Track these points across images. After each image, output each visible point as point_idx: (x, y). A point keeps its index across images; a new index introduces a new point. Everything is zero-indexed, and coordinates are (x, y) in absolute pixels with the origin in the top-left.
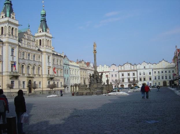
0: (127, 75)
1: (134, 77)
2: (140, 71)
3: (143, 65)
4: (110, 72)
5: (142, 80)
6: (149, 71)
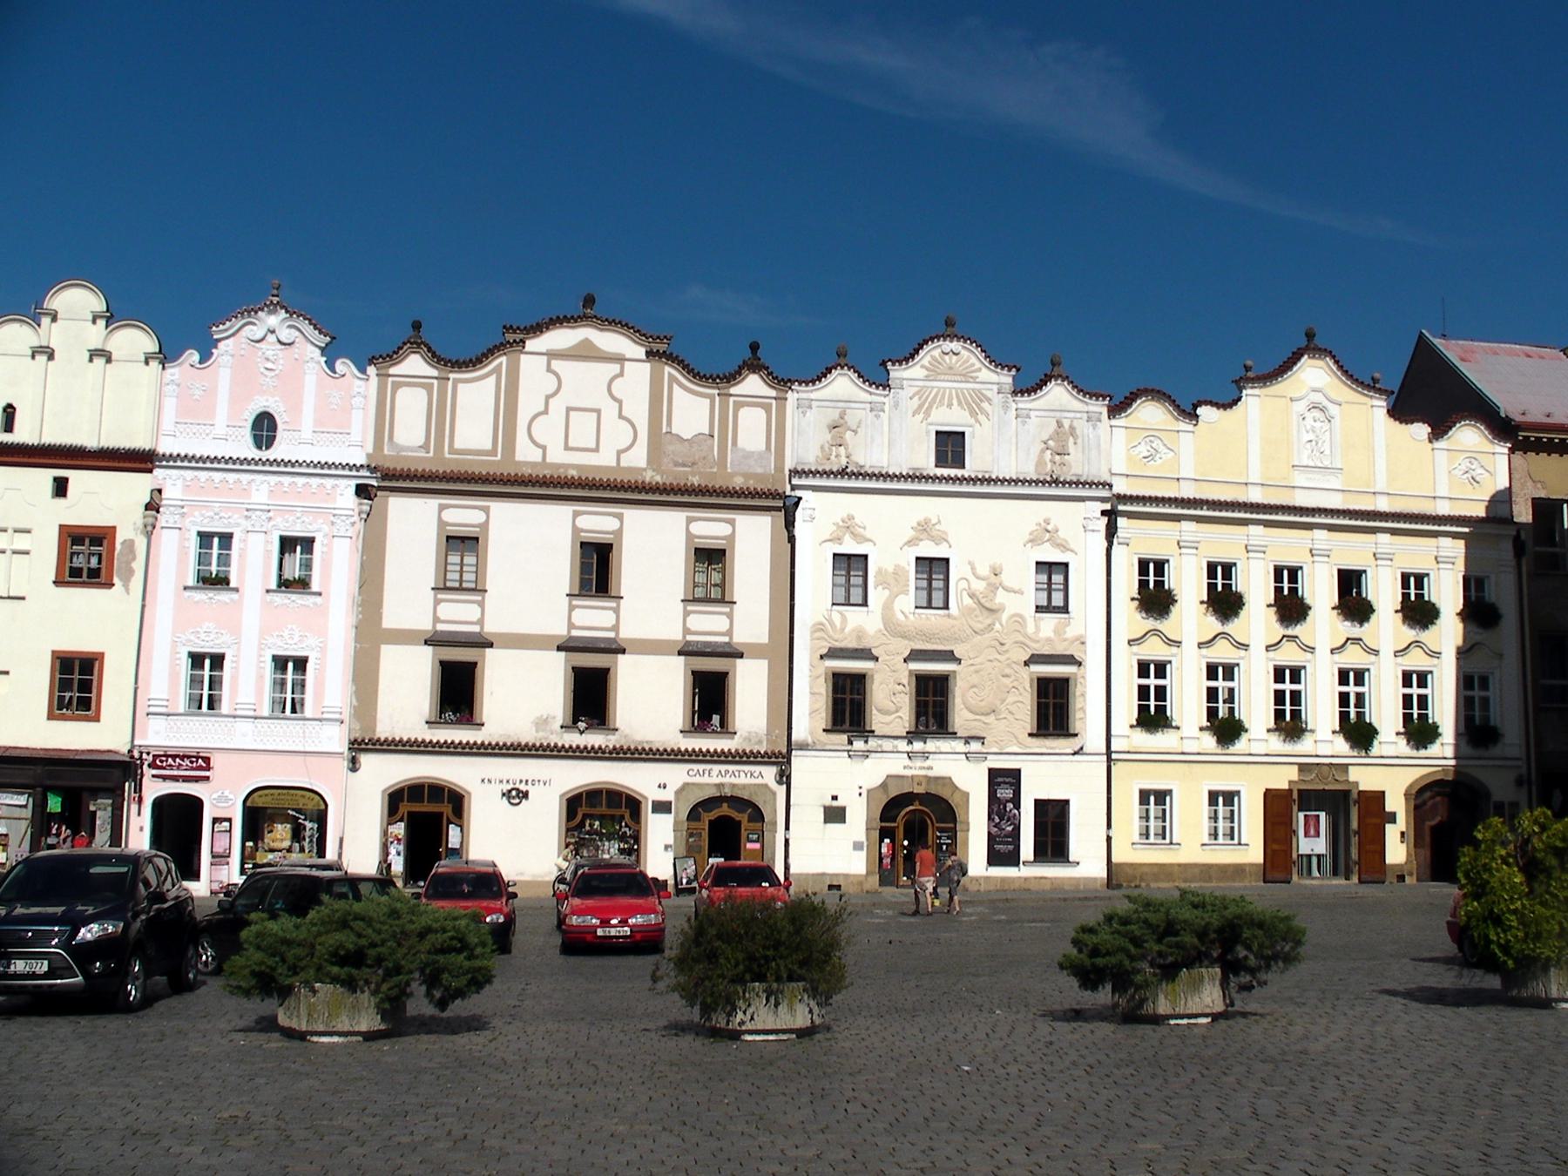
0: (562, 568)
1: (709, 624)
2: (848, 526)
3: (924, 409)
4: (171, 481)
5: (877, 720)
6: (1046, 533)
